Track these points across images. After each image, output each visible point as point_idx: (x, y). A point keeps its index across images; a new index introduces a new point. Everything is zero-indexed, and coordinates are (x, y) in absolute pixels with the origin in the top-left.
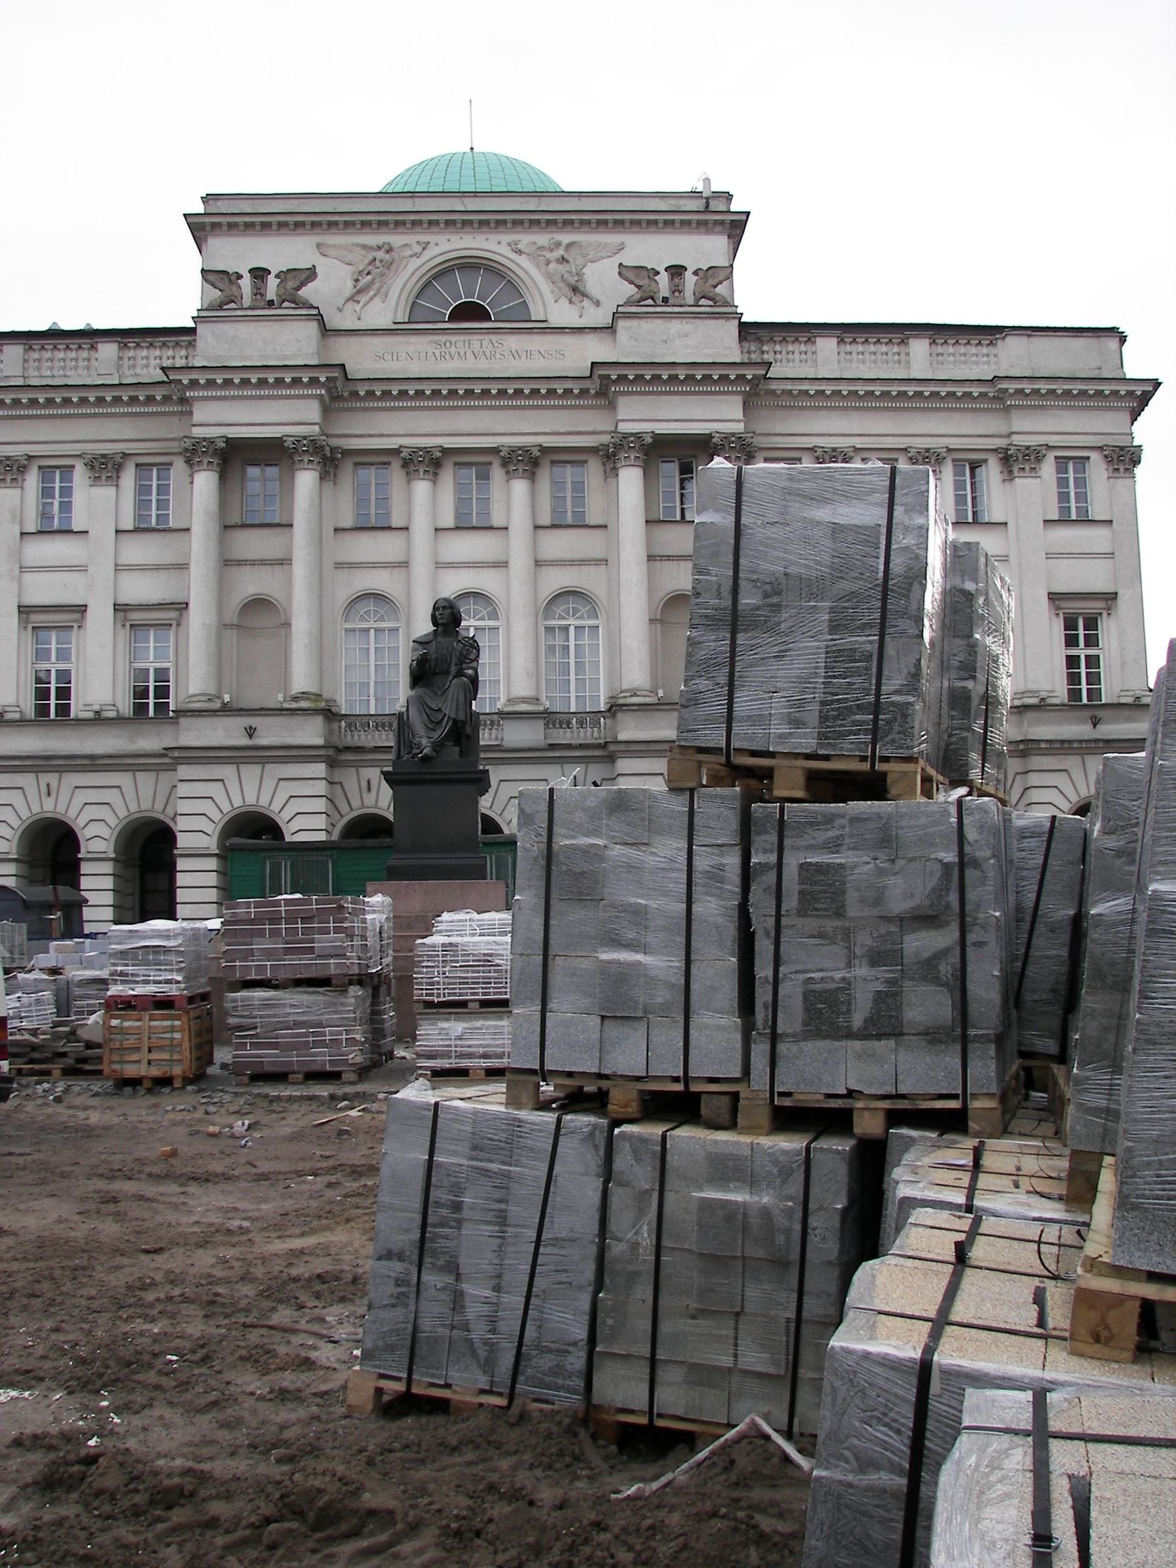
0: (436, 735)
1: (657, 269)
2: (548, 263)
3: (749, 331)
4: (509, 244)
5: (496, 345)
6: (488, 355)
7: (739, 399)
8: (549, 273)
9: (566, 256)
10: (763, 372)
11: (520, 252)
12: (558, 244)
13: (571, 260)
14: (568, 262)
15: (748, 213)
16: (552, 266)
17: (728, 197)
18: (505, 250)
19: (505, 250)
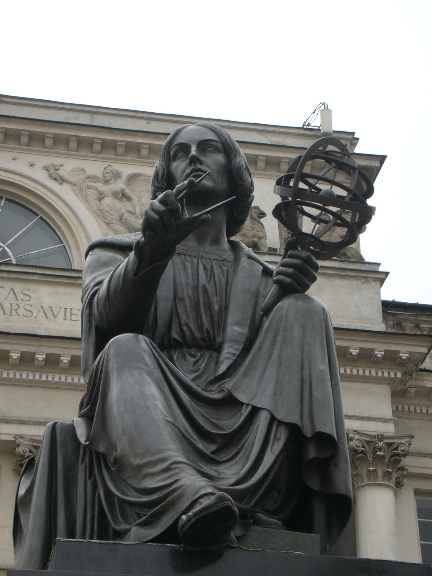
0: (230, 473)
1: (263, 208)
2: (101, 196)
3: (389, 307)
4: (46, 168)
5: (20, 296)
6: (7, 307)
7: (385, 391)
8: (102, 211)
9: (127, 191)
10: (425, 350)
11: (61, 180)
12: (117, 176)
13: (135, 198)
14: (129, 199)
15: (382, 159)
16: (108, 201)
17: (353, 140)
18: (41, 175)
19: (41, 175)
